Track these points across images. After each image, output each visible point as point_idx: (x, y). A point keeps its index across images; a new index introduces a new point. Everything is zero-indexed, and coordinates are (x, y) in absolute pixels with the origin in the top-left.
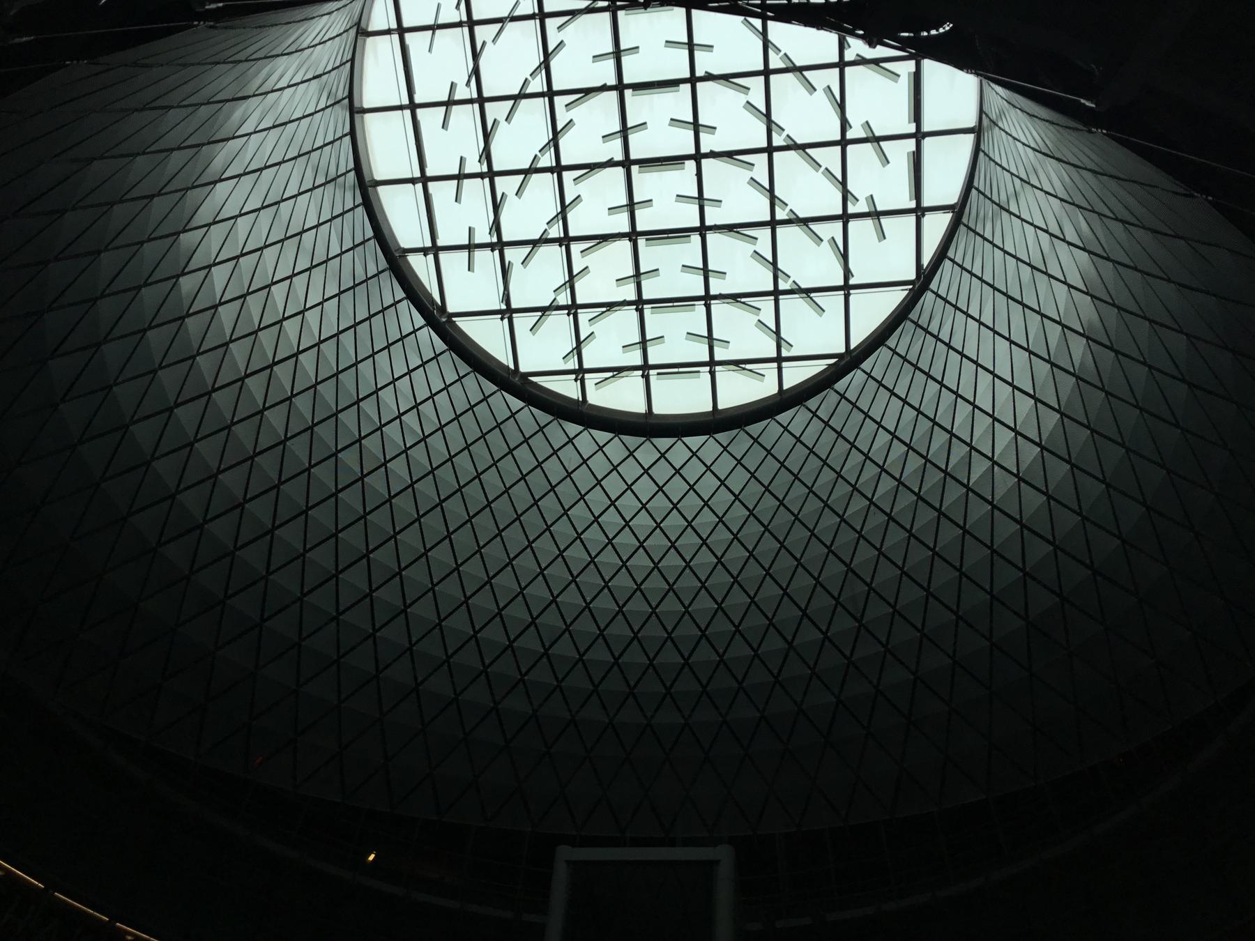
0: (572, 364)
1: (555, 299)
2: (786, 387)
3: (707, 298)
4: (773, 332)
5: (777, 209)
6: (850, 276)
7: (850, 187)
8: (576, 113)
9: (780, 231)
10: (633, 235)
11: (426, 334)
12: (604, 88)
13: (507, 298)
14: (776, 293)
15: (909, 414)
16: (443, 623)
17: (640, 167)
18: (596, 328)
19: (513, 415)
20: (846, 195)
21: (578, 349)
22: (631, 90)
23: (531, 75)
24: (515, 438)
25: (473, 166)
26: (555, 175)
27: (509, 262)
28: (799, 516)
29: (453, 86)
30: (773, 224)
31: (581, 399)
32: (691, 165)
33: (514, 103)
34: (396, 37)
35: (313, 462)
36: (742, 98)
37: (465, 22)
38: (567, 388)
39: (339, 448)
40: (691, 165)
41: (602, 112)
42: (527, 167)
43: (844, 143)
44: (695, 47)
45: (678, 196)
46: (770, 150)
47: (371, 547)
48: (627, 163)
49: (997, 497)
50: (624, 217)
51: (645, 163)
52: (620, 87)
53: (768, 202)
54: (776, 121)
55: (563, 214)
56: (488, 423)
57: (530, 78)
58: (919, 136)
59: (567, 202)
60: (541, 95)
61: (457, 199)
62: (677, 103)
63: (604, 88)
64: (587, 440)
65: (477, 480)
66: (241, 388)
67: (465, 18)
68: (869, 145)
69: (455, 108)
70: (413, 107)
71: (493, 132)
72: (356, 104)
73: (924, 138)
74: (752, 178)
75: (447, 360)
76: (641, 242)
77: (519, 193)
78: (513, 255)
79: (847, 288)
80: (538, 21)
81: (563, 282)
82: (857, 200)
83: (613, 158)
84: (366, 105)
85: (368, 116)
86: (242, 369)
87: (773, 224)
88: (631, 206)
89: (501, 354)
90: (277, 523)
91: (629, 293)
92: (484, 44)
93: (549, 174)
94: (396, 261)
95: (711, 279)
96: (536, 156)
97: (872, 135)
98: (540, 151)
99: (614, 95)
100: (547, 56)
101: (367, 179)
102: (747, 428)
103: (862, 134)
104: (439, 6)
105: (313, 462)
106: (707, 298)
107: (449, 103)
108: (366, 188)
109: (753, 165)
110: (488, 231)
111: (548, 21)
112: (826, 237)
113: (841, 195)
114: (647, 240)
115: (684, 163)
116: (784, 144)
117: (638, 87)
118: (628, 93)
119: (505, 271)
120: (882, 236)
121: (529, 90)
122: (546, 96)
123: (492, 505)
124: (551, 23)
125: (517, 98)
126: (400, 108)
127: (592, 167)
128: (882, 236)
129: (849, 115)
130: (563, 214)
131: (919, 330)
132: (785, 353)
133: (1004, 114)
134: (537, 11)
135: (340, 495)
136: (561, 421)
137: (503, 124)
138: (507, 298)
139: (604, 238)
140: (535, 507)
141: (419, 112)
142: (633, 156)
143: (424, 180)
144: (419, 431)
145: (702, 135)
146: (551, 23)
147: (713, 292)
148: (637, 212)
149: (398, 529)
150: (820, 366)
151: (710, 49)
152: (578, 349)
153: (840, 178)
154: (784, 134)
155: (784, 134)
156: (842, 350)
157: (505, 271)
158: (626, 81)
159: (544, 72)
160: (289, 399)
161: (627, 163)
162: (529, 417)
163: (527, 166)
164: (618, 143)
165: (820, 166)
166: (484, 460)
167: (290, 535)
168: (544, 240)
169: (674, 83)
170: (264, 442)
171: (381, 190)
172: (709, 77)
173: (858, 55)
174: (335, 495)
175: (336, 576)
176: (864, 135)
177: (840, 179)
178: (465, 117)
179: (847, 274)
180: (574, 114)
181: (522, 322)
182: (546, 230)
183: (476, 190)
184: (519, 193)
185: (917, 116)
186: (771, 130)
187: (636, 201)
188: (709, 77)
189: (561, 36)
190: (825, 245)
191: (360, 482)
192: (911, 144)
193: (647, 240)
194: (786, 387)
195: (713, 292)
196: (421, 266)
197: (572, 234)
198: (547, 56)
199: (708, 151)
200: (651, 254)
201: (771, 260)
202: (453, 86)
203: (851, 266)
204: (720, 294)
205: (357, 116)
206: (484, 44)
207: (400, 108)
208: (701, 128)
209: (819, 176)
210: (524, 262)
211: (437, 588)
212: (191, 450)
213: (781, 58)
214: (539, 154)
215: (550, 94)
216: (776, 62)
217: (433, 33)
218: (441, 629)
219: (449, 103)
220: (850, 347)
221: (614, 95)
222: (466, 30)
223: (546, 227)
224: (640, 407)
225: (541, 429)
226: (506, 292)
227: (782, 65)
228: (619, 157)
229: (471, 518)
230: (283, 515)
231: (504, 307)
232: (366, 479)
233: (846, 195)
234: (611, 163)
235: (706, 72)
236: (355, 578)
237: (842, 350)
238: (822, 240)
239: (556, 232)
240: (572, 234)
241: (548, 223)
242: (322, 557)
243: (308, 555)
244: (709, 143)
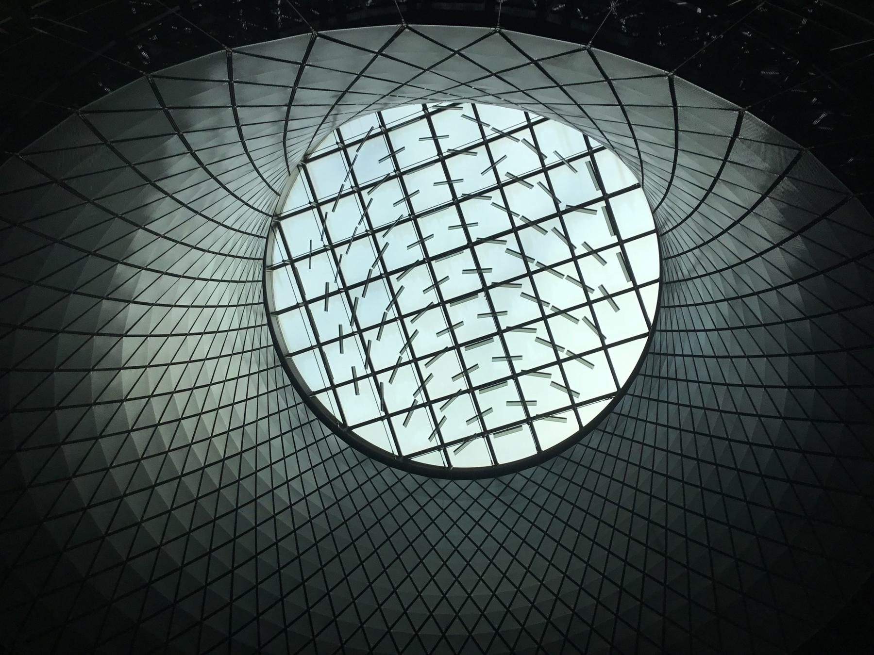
0: (436, 442)
1: (415, 400)
2: (584, 425)
3: (529, 420)
4: (564, 387)
5: (544, 307)
6: (574, 248)
7: (587, 283)
8: (432, 368)
9: (535, 277)
10: (485, 434)
11: (332, 439)
12: (447, 349)
13: (384, 407)
14: (559, 362)
15: (673, 408)
16: (365, 626)
17: (479, 390)
18: (445, 412)
19: (400, 480)
20: (586, 289)
21: (437, 430)
22: (449, 304)
23: (372, 267)
24: (402, 495)
25: (361, 371)
26: (442, 451)
27: (381, 383)
28: (621, 504)
29: (327, 285)
30: (515, 230)
31: (447, 466)
32: (526, 427)
33: (380, 329)
34: (317, 350)
35: (258, 523)
36: (533, 336)
37: (355, 332)
38: (435, 460)
39: (276, 512)
40: (526, 427)
41: (420, 277)
42: (380, 322)
43: (575, 259)
44: (497, 314)
45: (493, 358)
46: (559, 362)
47: (305, 578)
48: (443, 303)
49: (750, 436)
50: (447, 336)
51: (454, 301)
52: (457, 347)
53: (567, 395)
54: (543, 300)
55: (423, 386)
56: (381, 488)
57: (372, 268)
58: (621, 243)
59: (424, 379)
60: (395, 320)
61: (341, 351)
62: (480, 304)
63: (447, 349)
64: (453, 489)
65: (378, 524)
66: (202, 475)
67: (341, 286)
68: (591, 256)
69: (345, 340)
70: (320, 345)
71: (356, 305)
72: (271, 310)
73: (607, 194)
74: (537, 338)
75: (349, 452)
76: (477, 392)
77: (378, 338)
78: (383, 378)
79: (605, 348)
80: (385, 279)
81: (418, 388)
82: (594, 290)
83: (461, 390)
84: (291, 352)
85: (280, 316)
86: (202, 462)
87: (515, 230)
88: (422, 241)
89: (387, 446)
90: (236, 565)
91: (476, 428)
92: (341, 256)
93: (423, 408)
94: (309, 399)
95: (529, 407)
96: (385, 313)
97: (607, 295)
98: (386, 309)
99: (453, 353)
100: (380, 252)
101: (284, 352)
102: (562, 455)
103: (585, 251)
104: (311, 241)
105: (258, 523)
106: (529, 420)
107: (341, 338)
108: (271, 315)
109: (536, 329)
110: (364, 367)
111: (420, 363)
112: (580, 317)
113: (582, 289)
114: (494, 434)
115: (493, 338)
116: (567, 356)
117: (453, 301)
118: (448, 306)
119: (380, 389)
120: (617, 308)
121: (373, 276)
122: (341, 149)
123: (391, 539)
124: (379, 236)
125: (381, 325)
126: (312, 348)
127: (436, 354)
128: (617, 308)
129: (573, 241)
130: (423, 386)
131: (670, 382)
132: (577, 401)
133: (669, 220)
134: (383, 272)
135: (279, 544)
136: (434, 479)
137: (361, 299)
138: (384, 407)
139: (466, 440)
140: (422, 536)
141: (324, 348)
142: (460, 342)
143: (320, 345)
144: (333, 497)
145: (529, 408)
146: (379, 236)
147: (532, 415)
148: (484, 418)
149: (324, 563)
150: (605, 403)
151: (506, 313)
152: (437, 430)
153: (578, 279)
154: (565, 351)
155: (565, 351)
156: (615, 390)
157: (380, 389)
158: (445, 299)
159: (437, 436)
160: (238, 481)
161: (443, 303)
162: (410, 481)
163: (365, 279)
164: (433, 292)
165: (564, 275)
166: (381, 511)
167: (246, 573)
168: (415, 407)
169: (474, 294)
170: (221, 511)
171: (295, 358)
172: (495, 285)
173: (567, 206)
174: (276, 543)
175: (282, 600)
176: (586, 251)
177: (579, 280)
178: (352, 344)
179: (602, 338)
180: (403, 282)
181: (397, 421)
182: (400, 356)
183: (352, 344)
184: (378, 338)
185: (615, 230)
186: (572, 396)
187: (453, 324)
188: (509, 329)
189: (386, 240)
190: (581, 322)
191: (294, 534)
192: (618, 249)
193: (494, 434)
194: (584, 425)
195: (532, 415)
196: (326, 400)
197: (446, 441)
198: (380, 252)
199: (506, 328)
200: (471, 356)
201: (564, 385)
202: (327, 285)
203: (603, 332)
204: (537, 415)
205: (273, 318)
206: (356, 299)
207: (312, 348)
208: (527, 403)
209: (564, 281)
210: (391, 381)
211: (356, 601)
212: (169, 516)
213: (520, 219)
214: (386, 311)
215: (415, 360)
216: (563, 355)
217: (310, 259)
218: (363, 631)
219: (341, 338)
220: (619, 387)
221: (453, 353)
222: (357, 336)
223: (400, 355)
224: (487, 462)
225: (420, 486)
226: (383, 403)
227: (523, 223)
228: (450, 344)
229: (376, 550)
230: (239, 560)
231: (383, 414)
232: (297, 532)
233: (586, 289)
234: (431, 307)
235: (522, 370)
236: (296, 600)
237: (615, 390)
238: (578, 320)
239: (421, 399)
240: (446, 441)
241: (400, 352)
242: (270, 587)
243: (259, 586)
244: (533, 411)
